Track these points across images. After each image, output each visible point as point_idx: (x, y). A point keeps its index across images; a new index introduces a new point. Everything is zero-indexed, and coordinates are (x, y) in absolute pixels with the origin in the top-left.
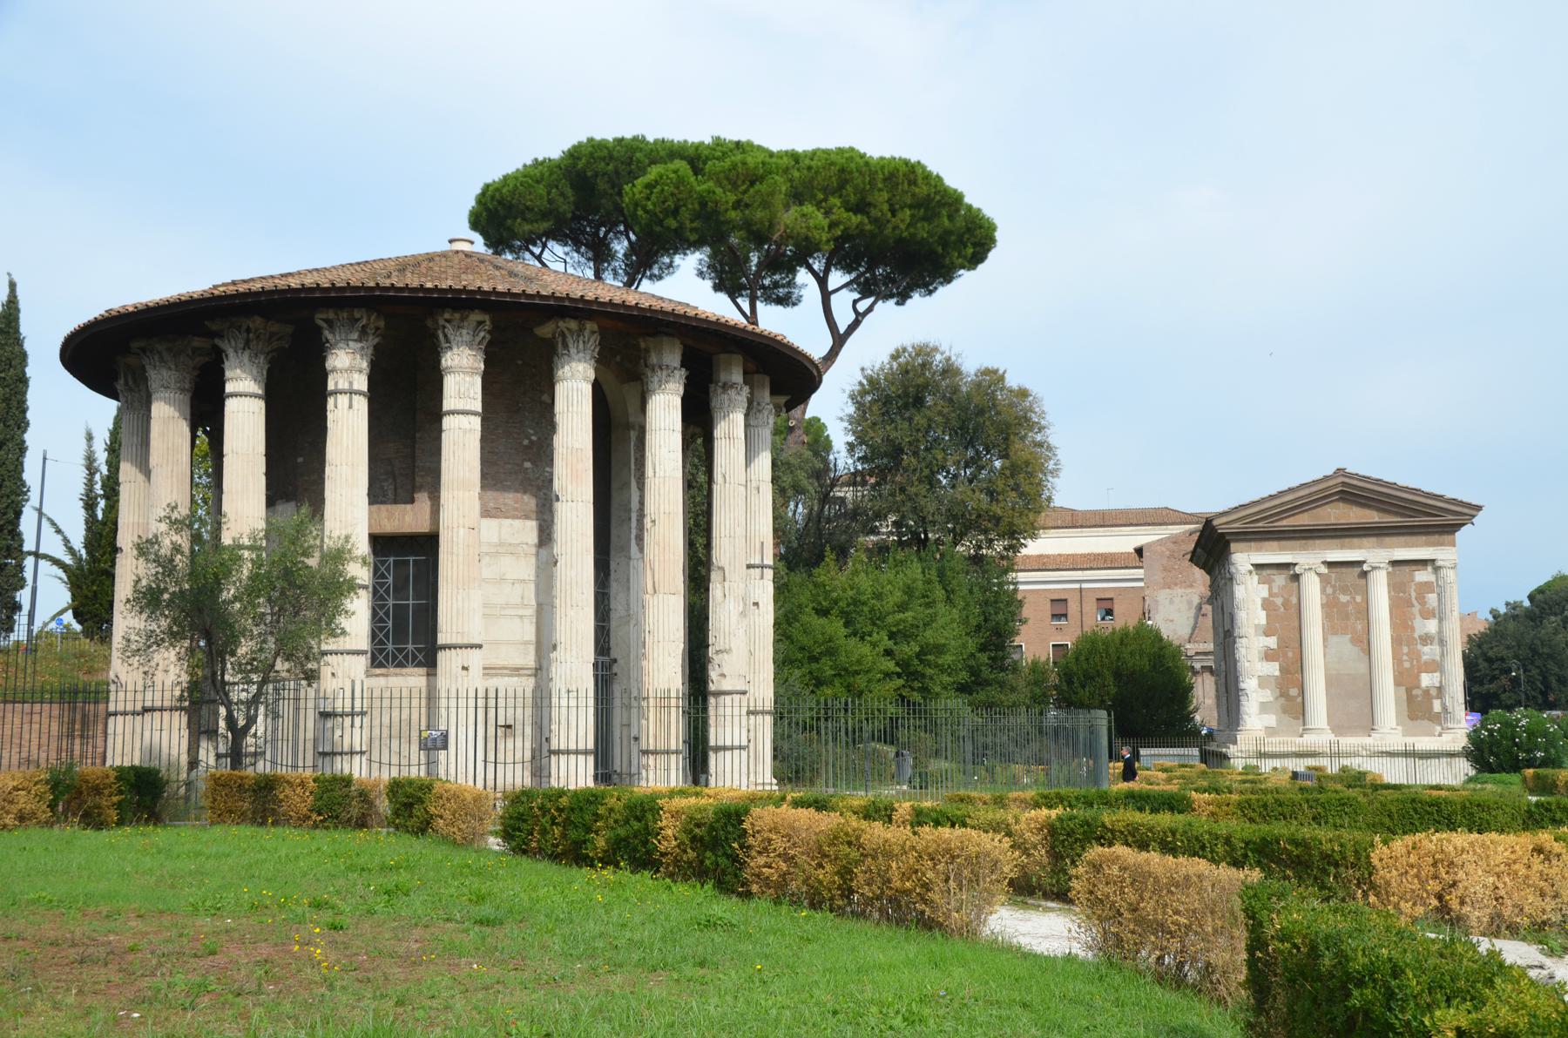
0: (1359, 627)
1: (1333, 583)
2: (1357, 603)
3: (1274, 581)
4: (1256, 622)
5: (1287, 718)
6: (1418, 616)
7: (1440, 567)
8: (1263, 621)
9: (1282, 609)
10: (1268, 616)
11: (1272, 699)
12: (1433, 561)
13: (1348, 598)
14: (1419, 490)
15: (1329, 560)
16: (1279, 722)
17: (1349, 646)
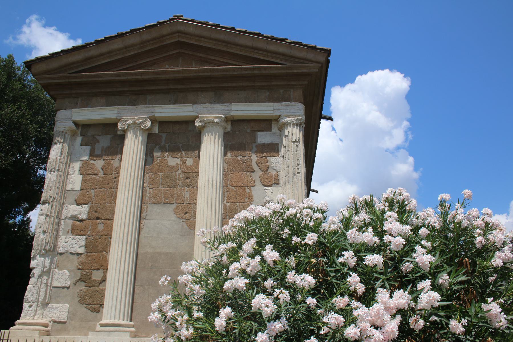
0: (187, 195)
1: (163, 143)
2: (187, 167)
3: (98, 142)
4: (69, 187)
5: (82, 310)
6: (258, 183)
7: (285, 125)
8: (77, 187)
9: (101, 174)
10: (84, 181)
11: (68, 283)
12: (277, 119)
13: (178, 161)
14: (259, 34)
15: (157, 115)
16: (72, 315)
17: (173, 218)
